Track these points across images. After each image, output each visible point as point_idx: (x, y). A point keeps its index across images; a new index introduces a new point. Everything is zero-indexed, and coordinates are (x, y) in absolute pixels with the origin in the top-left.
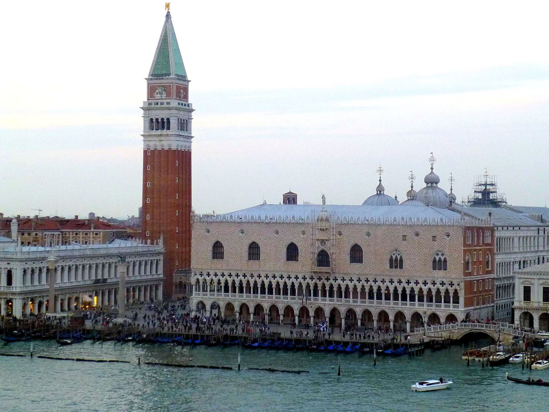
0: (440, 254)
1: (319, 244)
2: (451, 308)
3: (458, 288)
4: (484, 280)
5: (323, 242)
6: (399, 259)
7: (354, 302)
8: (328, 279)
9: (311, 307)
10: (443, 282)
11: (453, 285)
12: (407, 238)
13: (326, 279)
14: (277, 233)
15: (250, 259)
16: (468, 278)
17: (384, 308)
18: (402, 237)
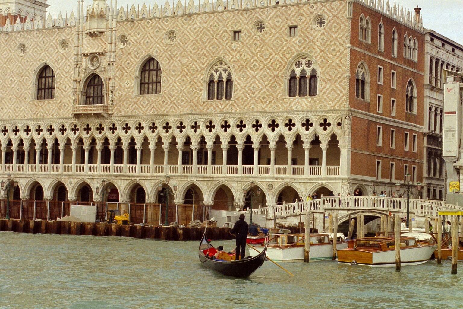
0: (304, 62)
1: (89, 63)
2: (324, 174)
3: (338, 131)
4: (400, 130)
5: (93, 57)
6: (225, 80)
7: (142, 170)
8: (100, 129)
9: (71, 183)
10: (308, 120)
11: (329, 124)
12: (241, 34)
13: (98, 129)
14: (23, 48)
16: (361, 114)
17: (194, 179)
18: (231, 34)
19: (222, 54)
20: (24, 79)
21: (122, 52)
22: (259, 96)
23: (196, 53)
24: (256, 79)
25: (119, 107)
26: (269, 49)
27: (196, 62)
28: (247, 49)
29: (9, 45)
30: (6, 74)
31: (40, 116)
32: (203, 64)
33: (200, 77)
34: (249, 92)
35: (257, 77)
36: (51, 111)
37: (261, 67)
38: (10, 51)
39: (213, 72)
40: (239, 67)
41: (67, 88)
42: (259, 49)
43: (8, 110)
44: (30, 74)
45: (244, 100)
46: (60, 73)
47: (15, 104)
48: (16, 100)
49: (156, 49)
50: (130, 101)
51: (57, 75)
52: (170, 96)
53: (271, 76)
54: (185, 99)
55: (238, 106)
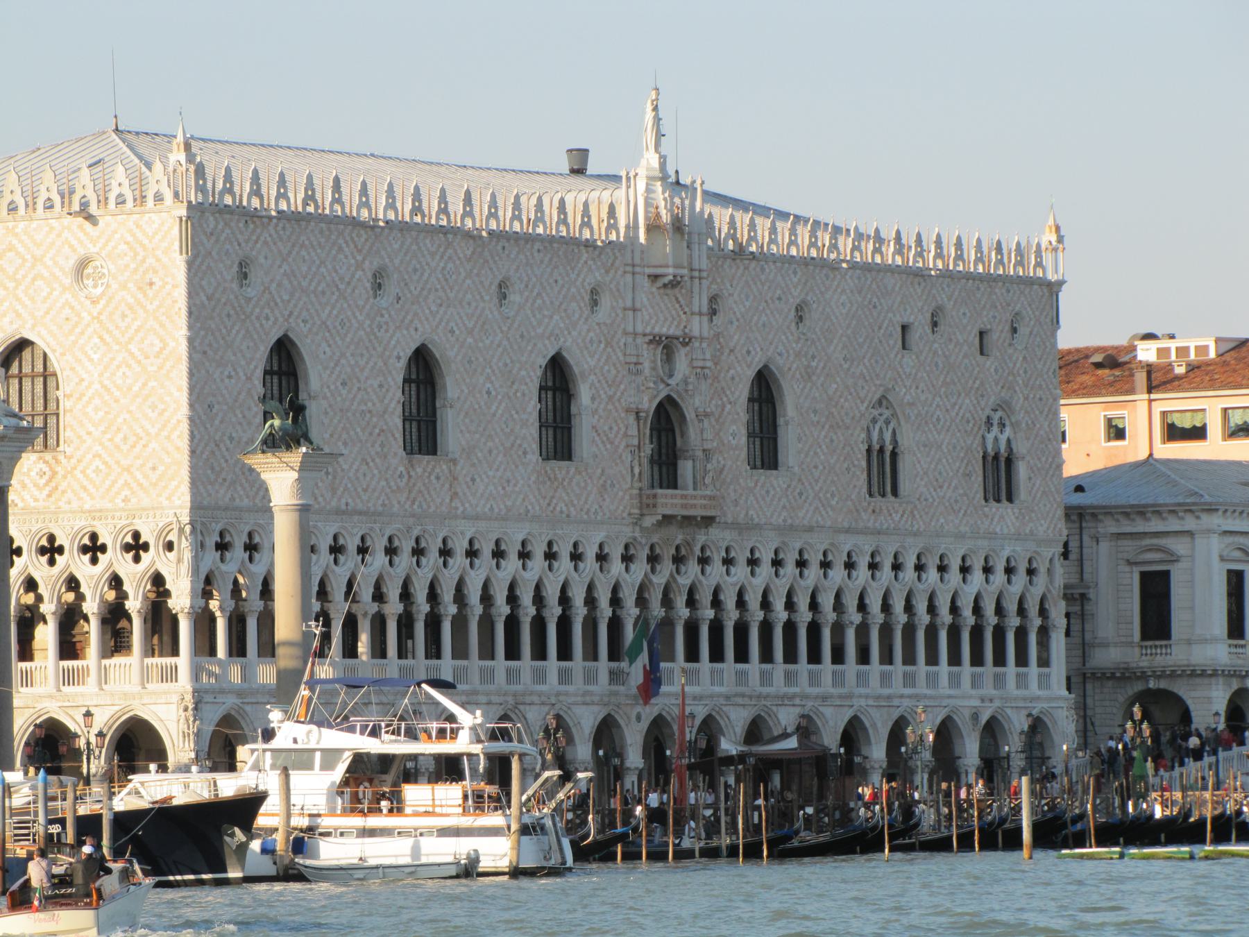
6: (889, 447)
9: (639, 718)
12: (914, 336)
18: (899, 329)
22: (948, 495)
23: (848, 369)
29: (478, 275)
36: (583, 499)
38: (480, 293)
47: (502, 470)
49: (781, 348)
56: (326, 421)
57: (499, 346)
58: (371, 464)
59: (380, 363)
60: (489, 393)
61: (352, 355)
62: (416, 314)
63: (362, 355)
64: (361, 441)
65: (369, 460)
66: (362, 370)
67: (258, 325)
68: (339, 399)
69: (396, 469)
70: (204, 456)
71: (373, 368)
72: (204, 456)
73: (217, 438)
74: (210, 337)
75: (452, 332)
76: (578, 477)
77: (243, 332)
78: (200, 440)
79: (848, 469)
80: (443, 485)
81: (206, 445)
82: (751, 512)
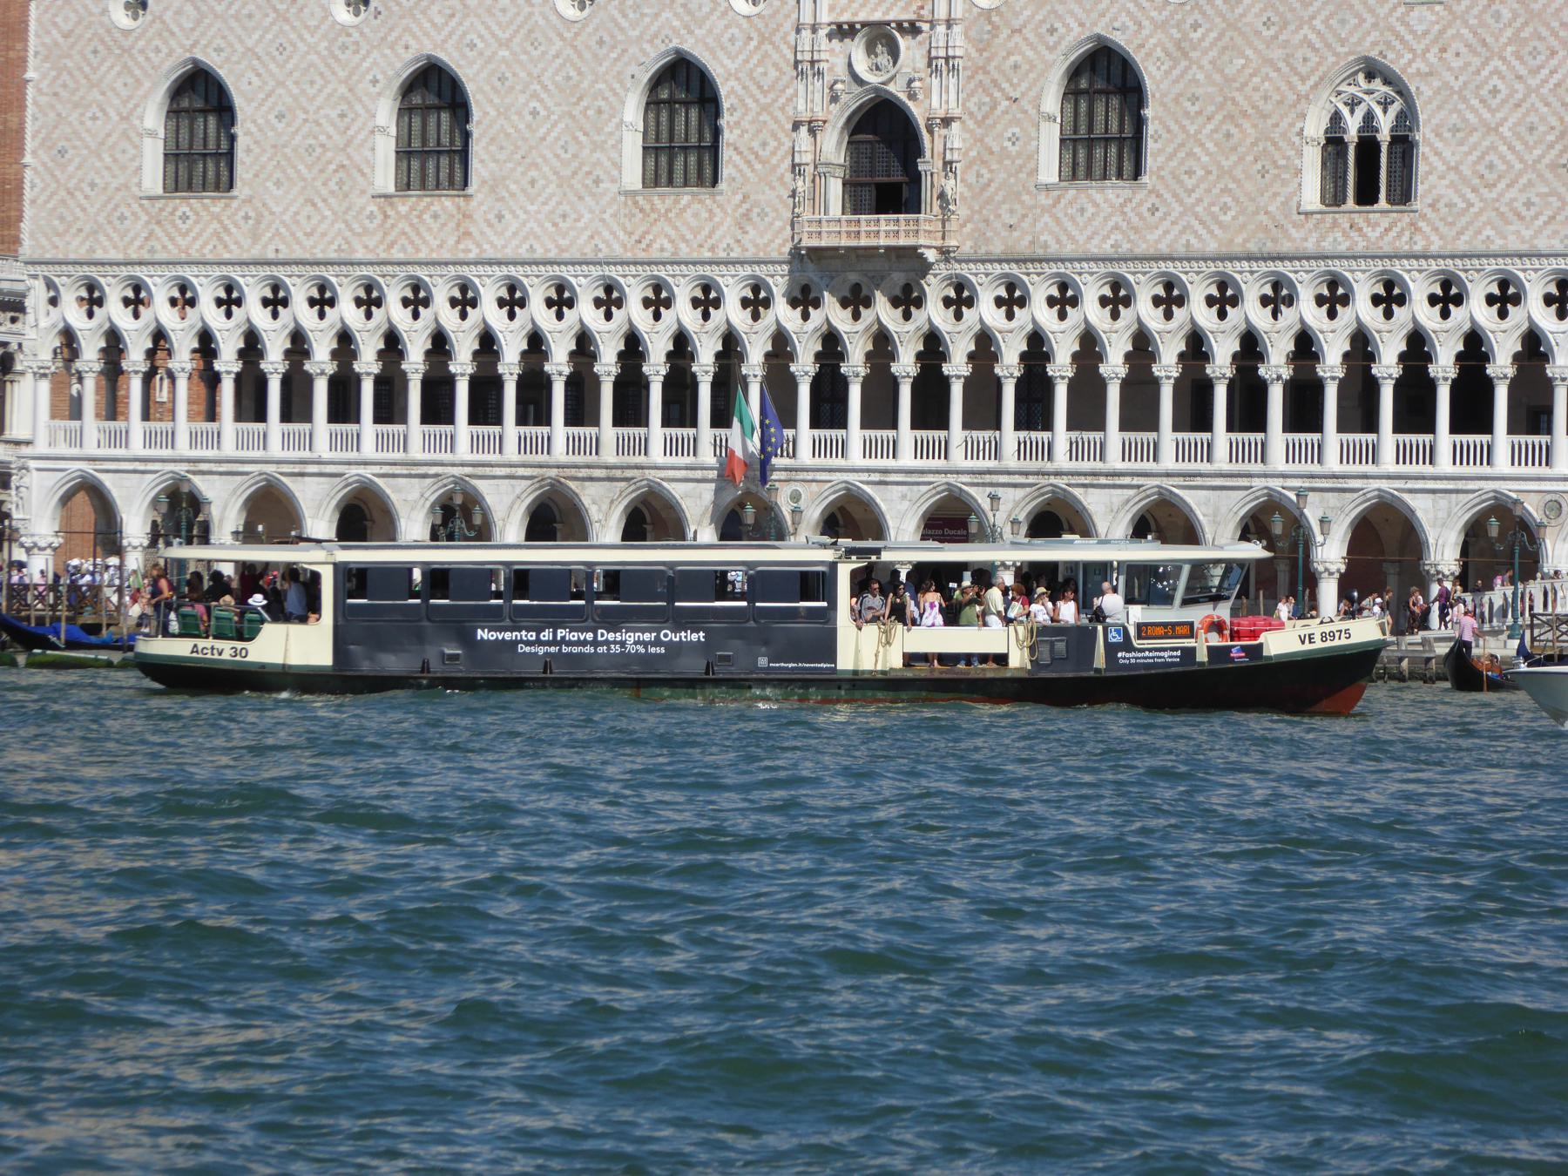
6: (1384, 136)
7: (1075, 451)
8: (908, 300)
15: (404, 185)
19: (1375, 44)
20: (587, 108)
21: (990, 22)
22: (1508, 196)
23: (1275, 37)
24: (1503, 138)
25: (982, 225)
26: (1545, 32)
27: (1278, 70)
28: (1465, 31)
30: (512, 88)
31: (662, 250)
32: (1303, 79)
33: (1292, 125)
34: (1476, 181)
35: (1505, 130)
36: (706, 232)
37: (1520, 96)
39: (1341, 107)
40: (1437, 92)
41: (769, 149)
42: (1509, 33)
43: (524, 224)
44: (612, 89)
45: (1455, 210)
46: (741, 92)
47: (552, 203)
48: (560, 186)
49: (1124, 18)
50: (1022, 203)
51: (727, 96)
52: (1180, 191)
53: (1552, 128)
54: (1236, 200)
55: (1436, 230)
56: (248, 160)
57: (557, 56)
58: (320, 204)
59: (343, 90)
60: (534, 113)
61: (296, 83)
62: (407, 29)
63: (312, 83)
64: (304, 180)
65: (318, 200)
66: (313, 99)
67: (141, 59)
68: (270, 134)
69: (363, 209)
70: (50, 206)
71: (330, 95)
72: (50, 206)
73: (71, 185)
74: (65, 77)
75: (472, 46)
76: (696, 206)
77: (118, 68)
78: (43, 190)
79: (1263, 173)
80: (444, 225)
81: (53, 194)
82: (1042, 238)
